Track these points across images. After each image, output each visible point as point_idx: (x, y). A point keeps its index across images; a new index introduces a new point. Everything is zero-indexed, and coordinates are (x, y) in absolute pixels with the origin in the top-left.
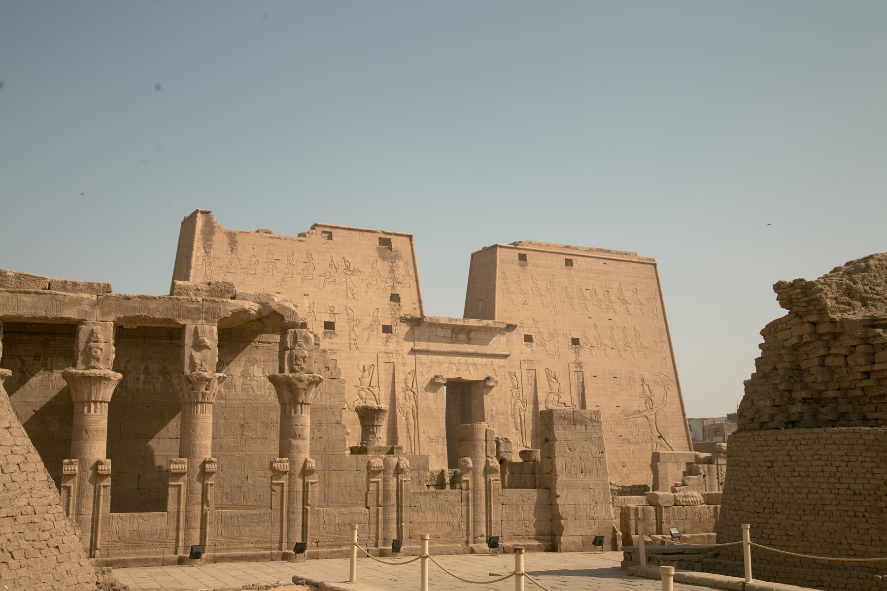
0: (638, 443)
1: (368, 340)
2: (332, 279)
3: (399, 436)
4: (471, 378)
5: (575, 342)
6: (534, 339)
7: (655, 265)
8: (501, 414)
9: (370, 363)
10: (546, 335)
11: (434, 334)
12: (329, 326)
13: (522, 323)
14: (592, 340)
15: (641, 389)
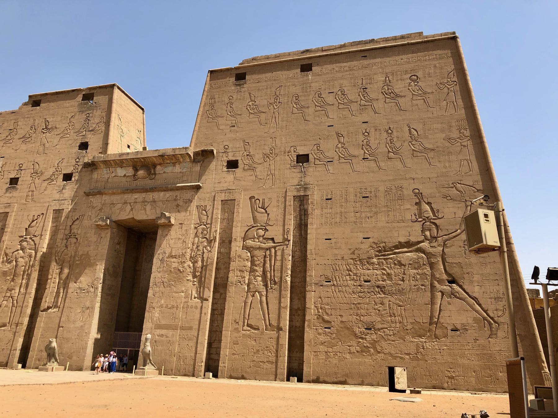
0: (401, 292)
1: (45, 190)
2: (30, 139)
3: (47, 287)
4: (144, 217)
5: (303, 159)
6: (240, 163)
7: (454, 39)
8: (175, 257)
9: (39, 213)
10: (258, 157)
11: (113, 175)
12: (14, 181)
13: (226, 148)
14: (331, 154)
15: (415, 209)
